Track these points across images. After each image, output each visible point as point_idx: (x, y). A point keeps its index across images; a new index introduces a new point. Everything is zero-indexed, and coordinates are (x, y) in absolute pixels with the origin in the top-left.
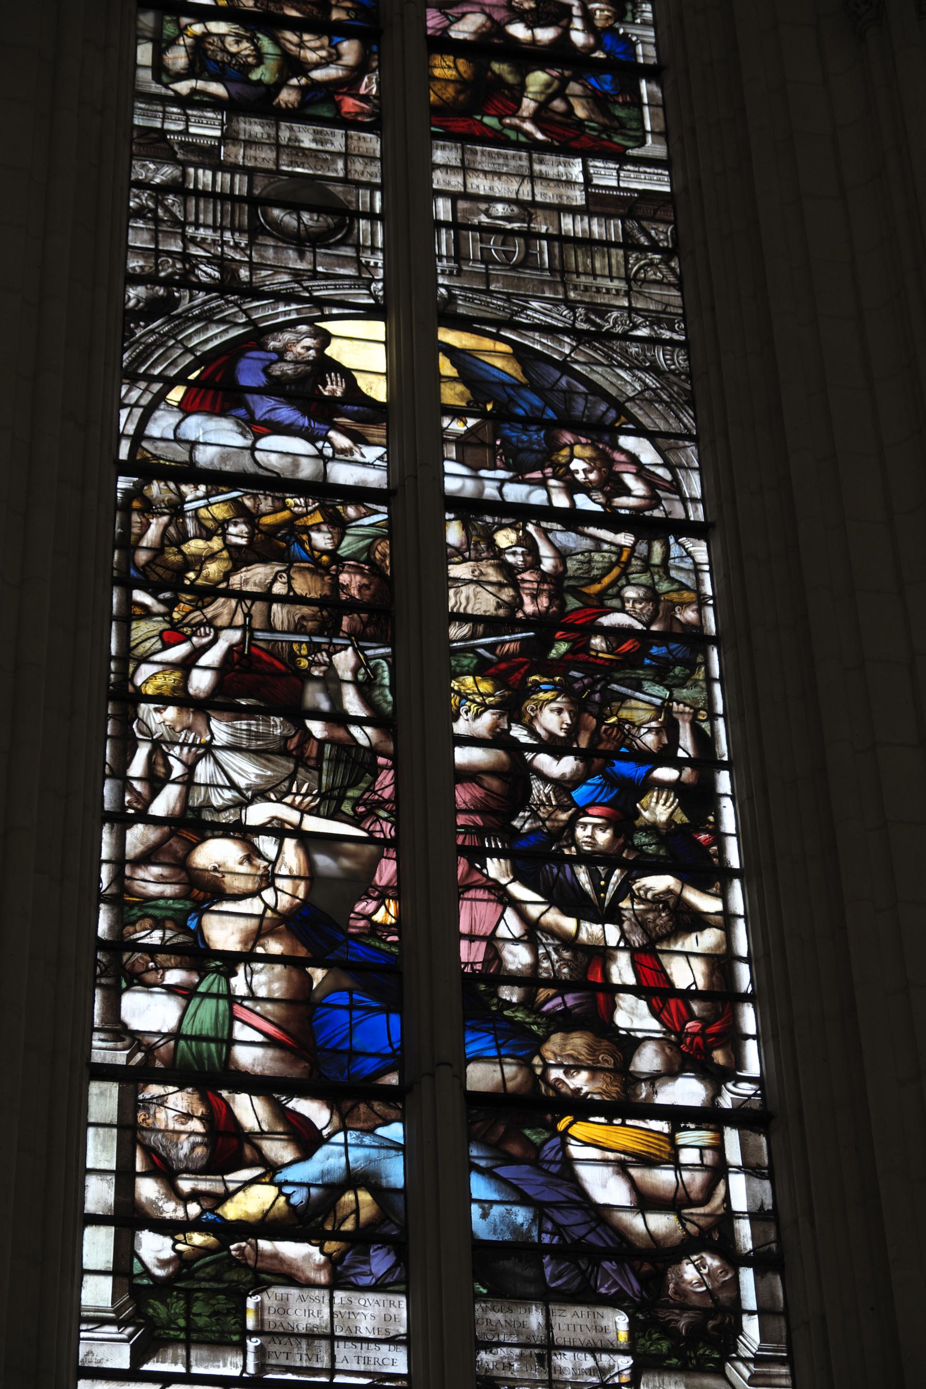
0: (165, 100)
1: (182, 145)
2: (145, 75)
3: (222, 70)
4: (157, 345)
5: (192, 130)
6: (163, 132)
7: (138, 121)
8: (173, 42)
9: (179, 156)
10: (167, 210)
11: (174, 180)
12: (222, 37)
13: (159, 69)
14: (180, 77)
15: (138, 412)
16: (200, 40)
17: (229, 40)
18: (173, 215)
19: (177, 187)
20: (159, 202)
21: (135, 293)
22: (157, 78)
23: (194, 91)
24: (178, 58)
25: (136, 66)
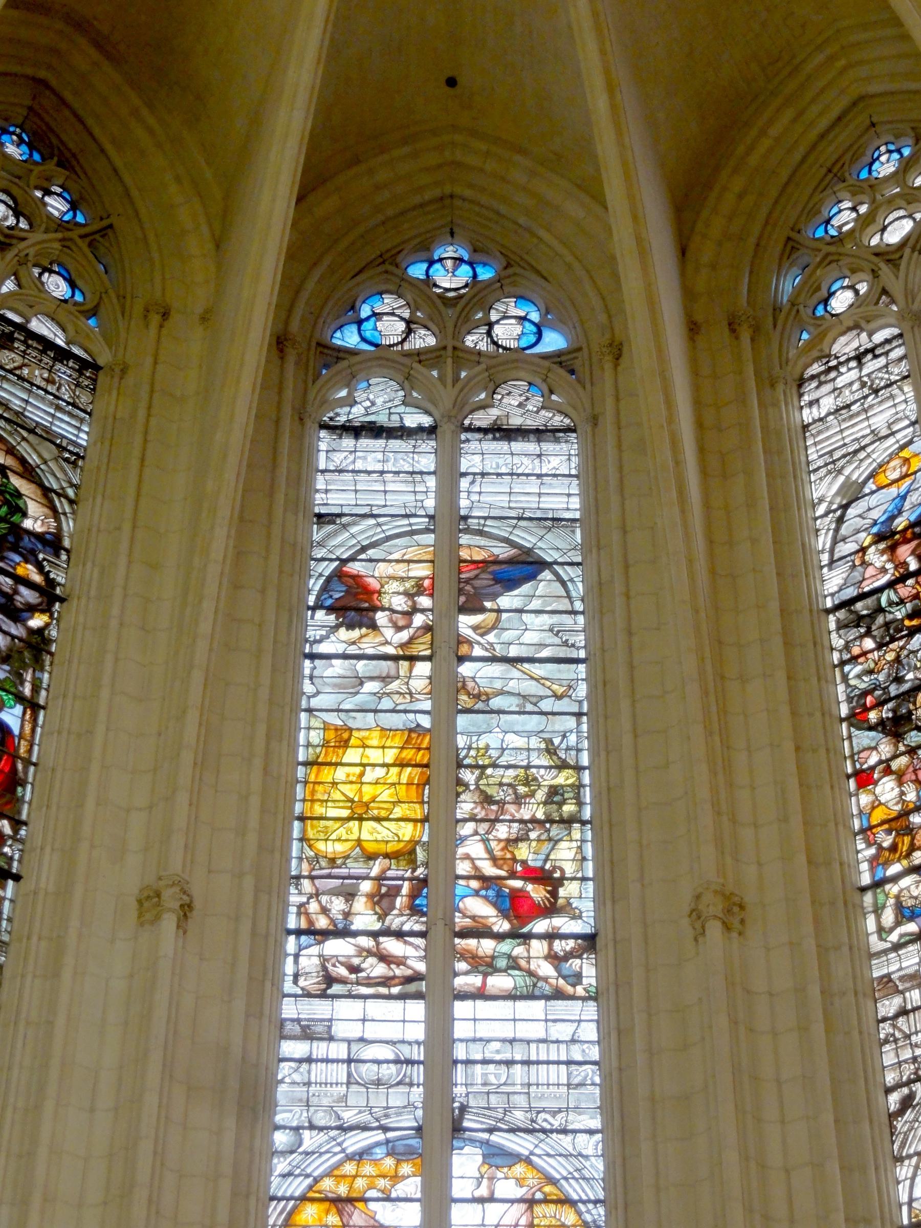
0: (885, 952)
1: (901, 979)
2: (874, 939)
3: (912, 912)
4: (910, 1130)
5: (904, 965)
6: (888, 976)
7: (876, 974)
8: (884, 907)
9: (900, 988)
10: (900, 1030)
11: (900, 1007)
12: (908, 889)
13: (881, 930)
14: (892, 930)
15: (908, 1182)
16: (897, 897)
17: (913, 887)
18: (904, 1032)
19: (903, 1012)
20: (894, 1026)
21: (894, 1099)
22: (881, 939)
23: (902, 936)
24: (888, 917)
25: (868, 935)
